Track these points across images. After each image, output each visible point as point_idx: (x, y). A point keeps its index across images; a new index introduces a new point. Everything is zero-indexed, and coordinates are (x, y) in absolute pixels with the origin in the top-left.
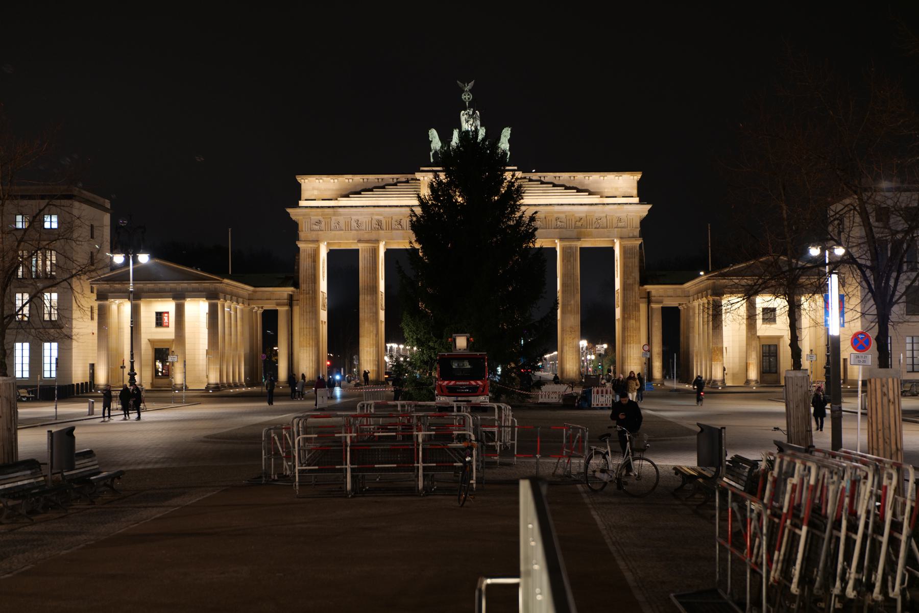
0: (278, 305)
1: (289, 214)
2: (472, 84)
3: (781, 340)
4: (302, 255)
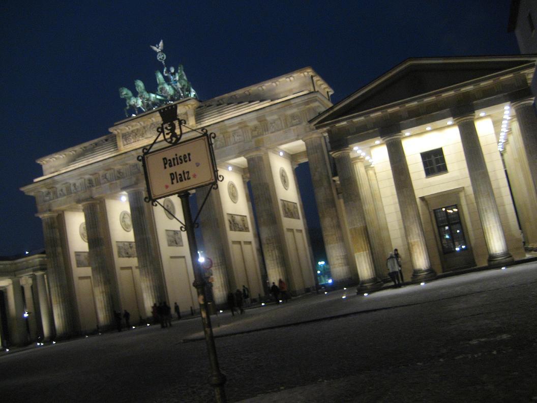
0: (35, 271)
1: (23, 193)
2: (161, 44)
3: (462, 195)
4: (44, 224)
